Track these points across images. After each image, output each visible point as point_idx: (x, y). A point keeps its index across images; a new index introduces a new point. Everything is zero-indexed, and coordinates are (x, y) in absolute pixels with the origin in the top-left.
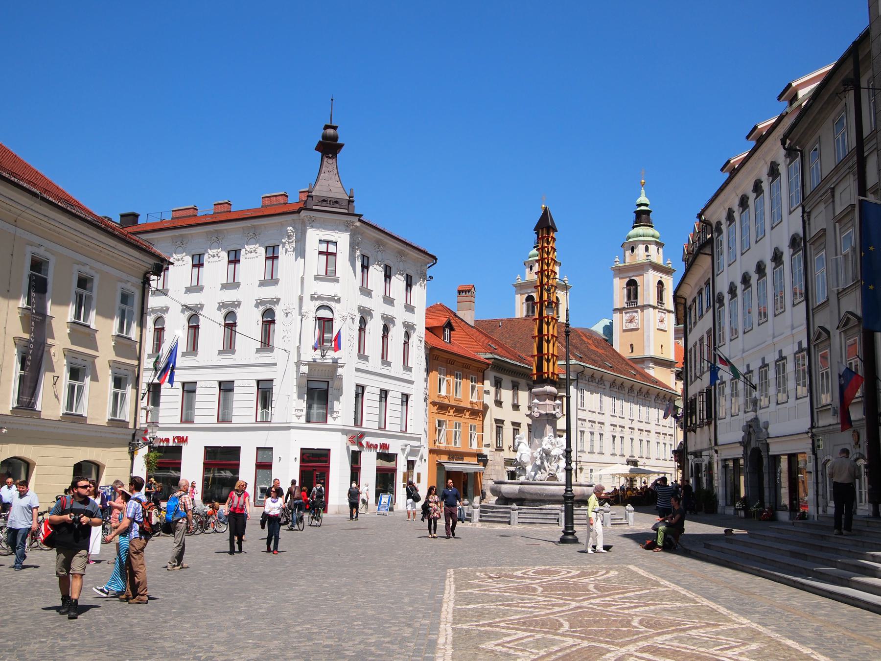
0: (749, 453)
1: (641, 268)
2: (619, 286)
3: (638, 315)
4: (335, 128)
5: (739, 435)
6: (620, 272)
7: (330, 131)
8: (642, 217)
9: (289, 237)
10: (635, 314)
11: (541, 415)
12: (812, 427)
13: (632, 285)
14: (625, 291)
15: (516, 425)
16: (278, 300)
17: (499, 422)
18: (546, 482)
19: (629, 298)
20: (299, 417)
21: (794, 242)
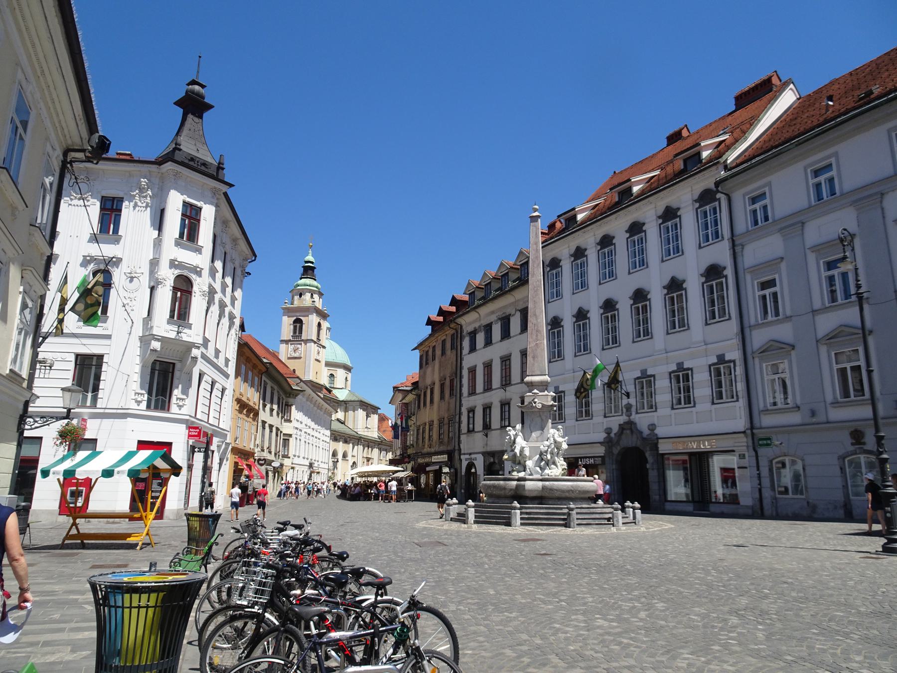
0: (616, 451)
1: (307, 311)
2: (287, 322)
3: (302, 347)
4: (203, 86)
5: (601, 436)
6: (288, 311)
7: (197, 88)
8: (308, 271)
9: (142, 190)
10: (299, 346)
11: (543, 405)
12: (752, 427)
13: (298, 322)
14: (292, 327)
15: (271, 426)
16: (120, 260)
17: (264, 422)
18: (560, 477)
19: (295, 332)
20: (139, 403)
21: (713, 272)
